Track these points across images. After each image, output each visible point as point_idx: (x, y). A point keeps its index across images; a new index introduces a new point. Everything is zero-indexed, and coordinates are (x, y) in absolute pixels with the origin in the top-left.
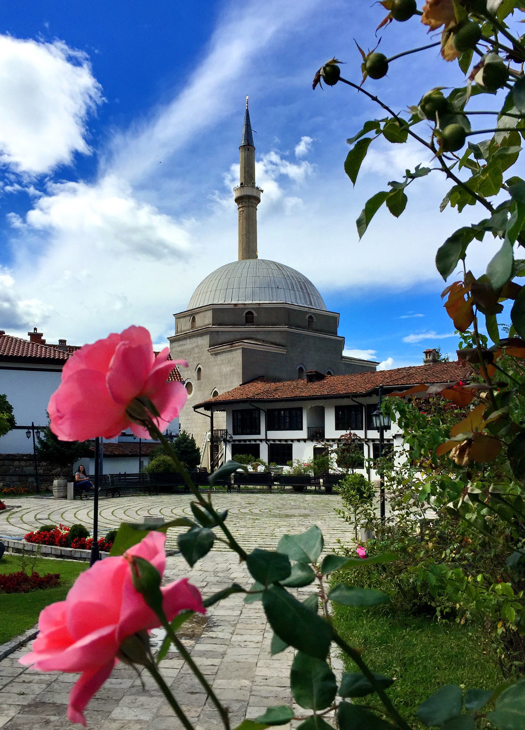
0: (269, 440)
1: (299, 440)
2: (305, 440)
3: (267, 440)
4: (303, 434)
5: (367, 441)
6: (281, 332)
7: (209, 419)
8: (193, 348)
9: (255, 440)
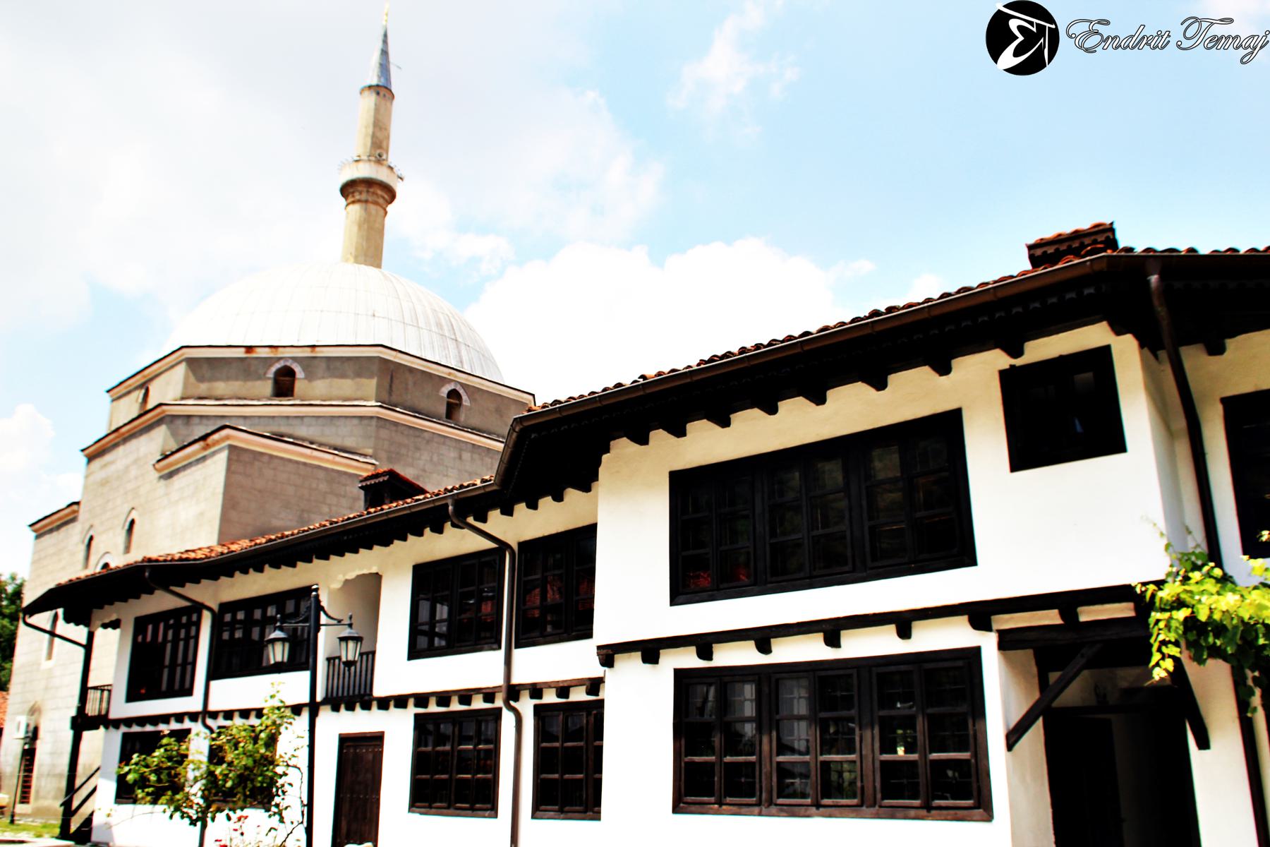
0: (214, 715)
5: (513, 692)
6: (361, 418)
7: (82, 651)
8: (127, 468)
9: (179, 717)
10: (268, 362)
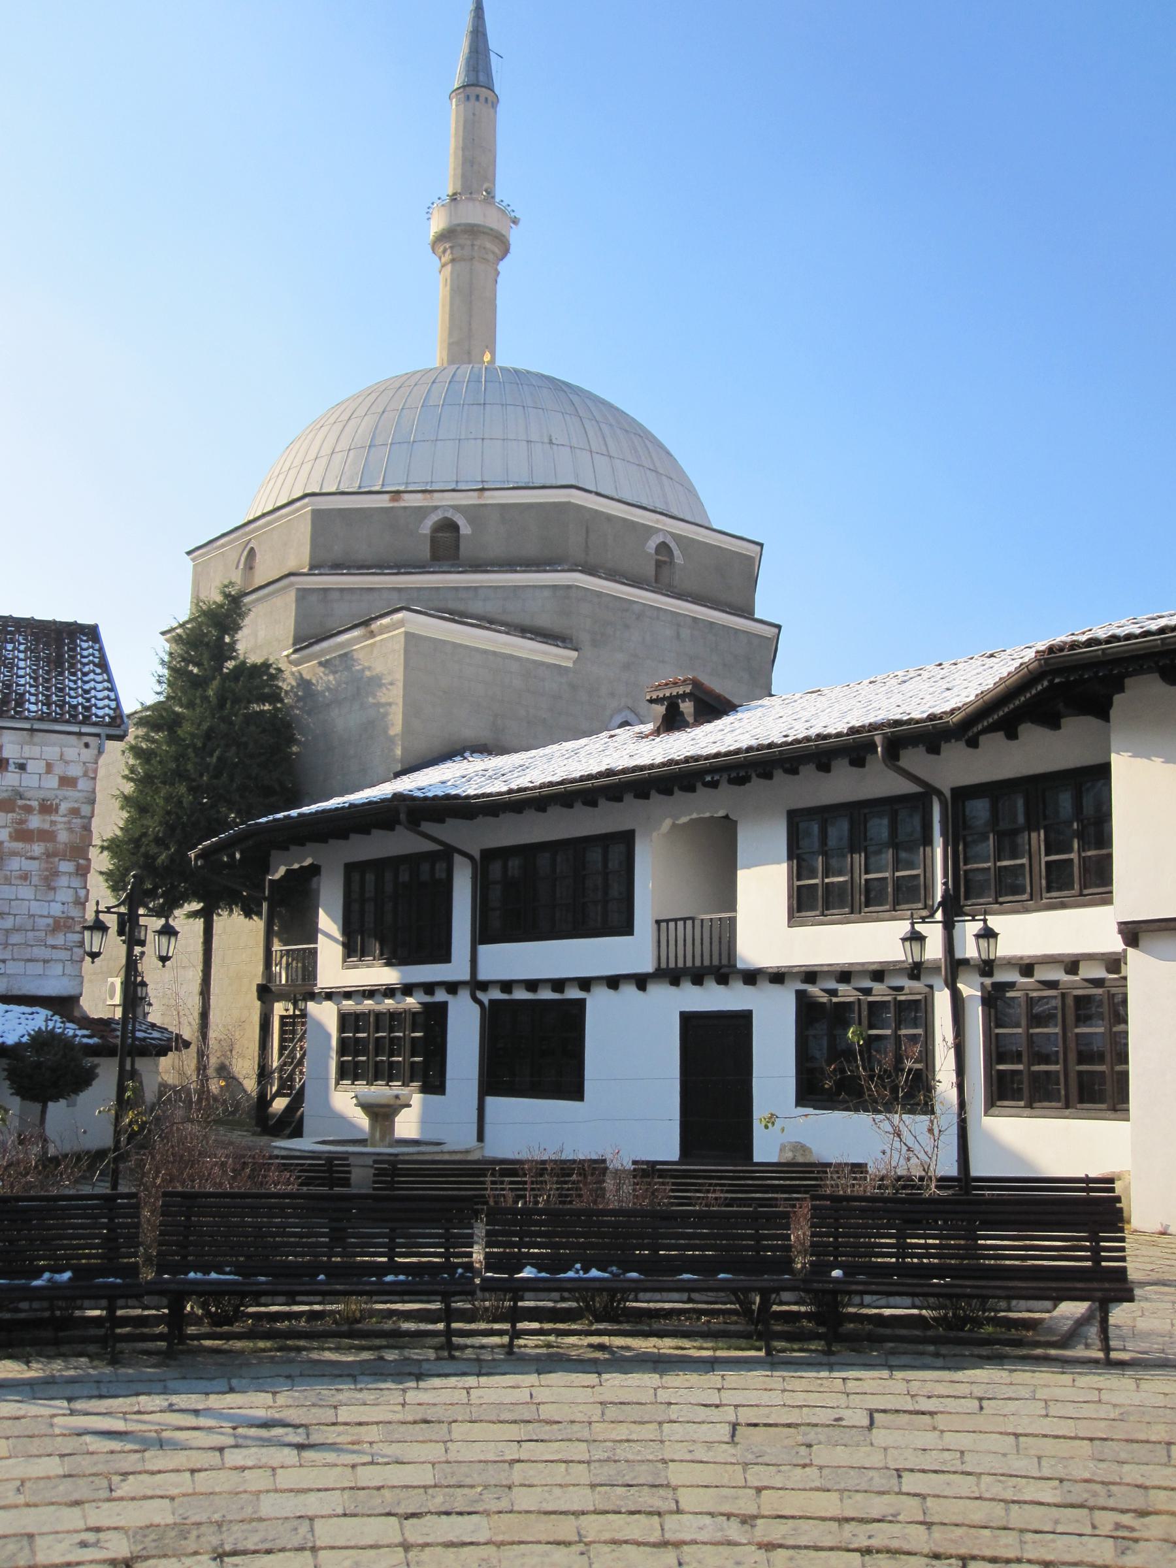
0: (484, 986)
1: (614, 982)
2: (641, 981)
3: (477, 985)
4: (634, 952)
9: (429, 988)
10: (421, 512)
